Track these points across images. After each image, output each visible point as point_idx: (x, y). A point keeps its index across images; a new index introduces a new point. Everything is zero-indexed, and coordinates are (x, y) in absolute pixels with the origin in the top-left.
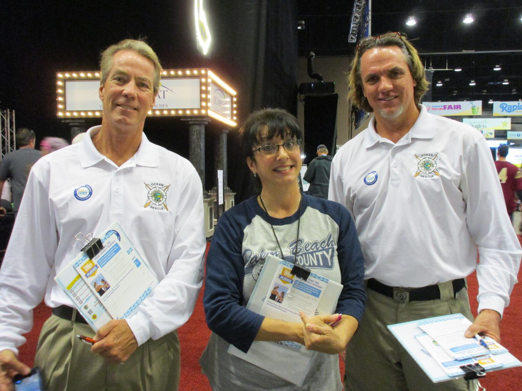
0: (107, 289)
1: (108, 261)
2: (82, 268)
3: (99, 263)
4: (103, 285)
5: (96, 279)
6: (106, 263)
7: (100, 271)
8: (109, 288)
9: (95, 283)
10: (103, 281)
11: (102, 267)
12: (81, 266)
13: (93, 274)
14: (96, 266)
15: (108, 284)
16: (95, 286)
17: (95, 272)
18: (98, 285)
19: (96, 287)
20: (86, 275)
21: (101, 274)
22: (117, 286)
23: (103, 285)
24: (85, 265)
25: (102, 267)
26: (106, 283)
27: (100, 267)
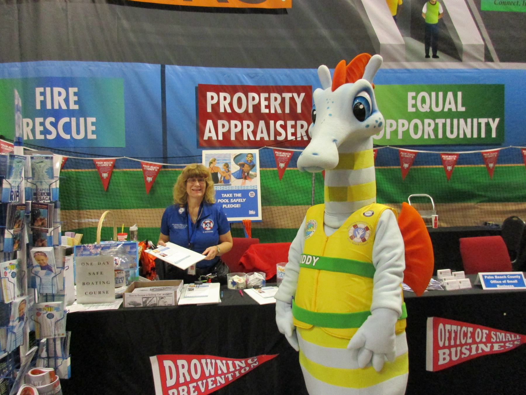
9: (215, 160)
18: (217, 165)
19: (212, 165)
26: (229, 171)
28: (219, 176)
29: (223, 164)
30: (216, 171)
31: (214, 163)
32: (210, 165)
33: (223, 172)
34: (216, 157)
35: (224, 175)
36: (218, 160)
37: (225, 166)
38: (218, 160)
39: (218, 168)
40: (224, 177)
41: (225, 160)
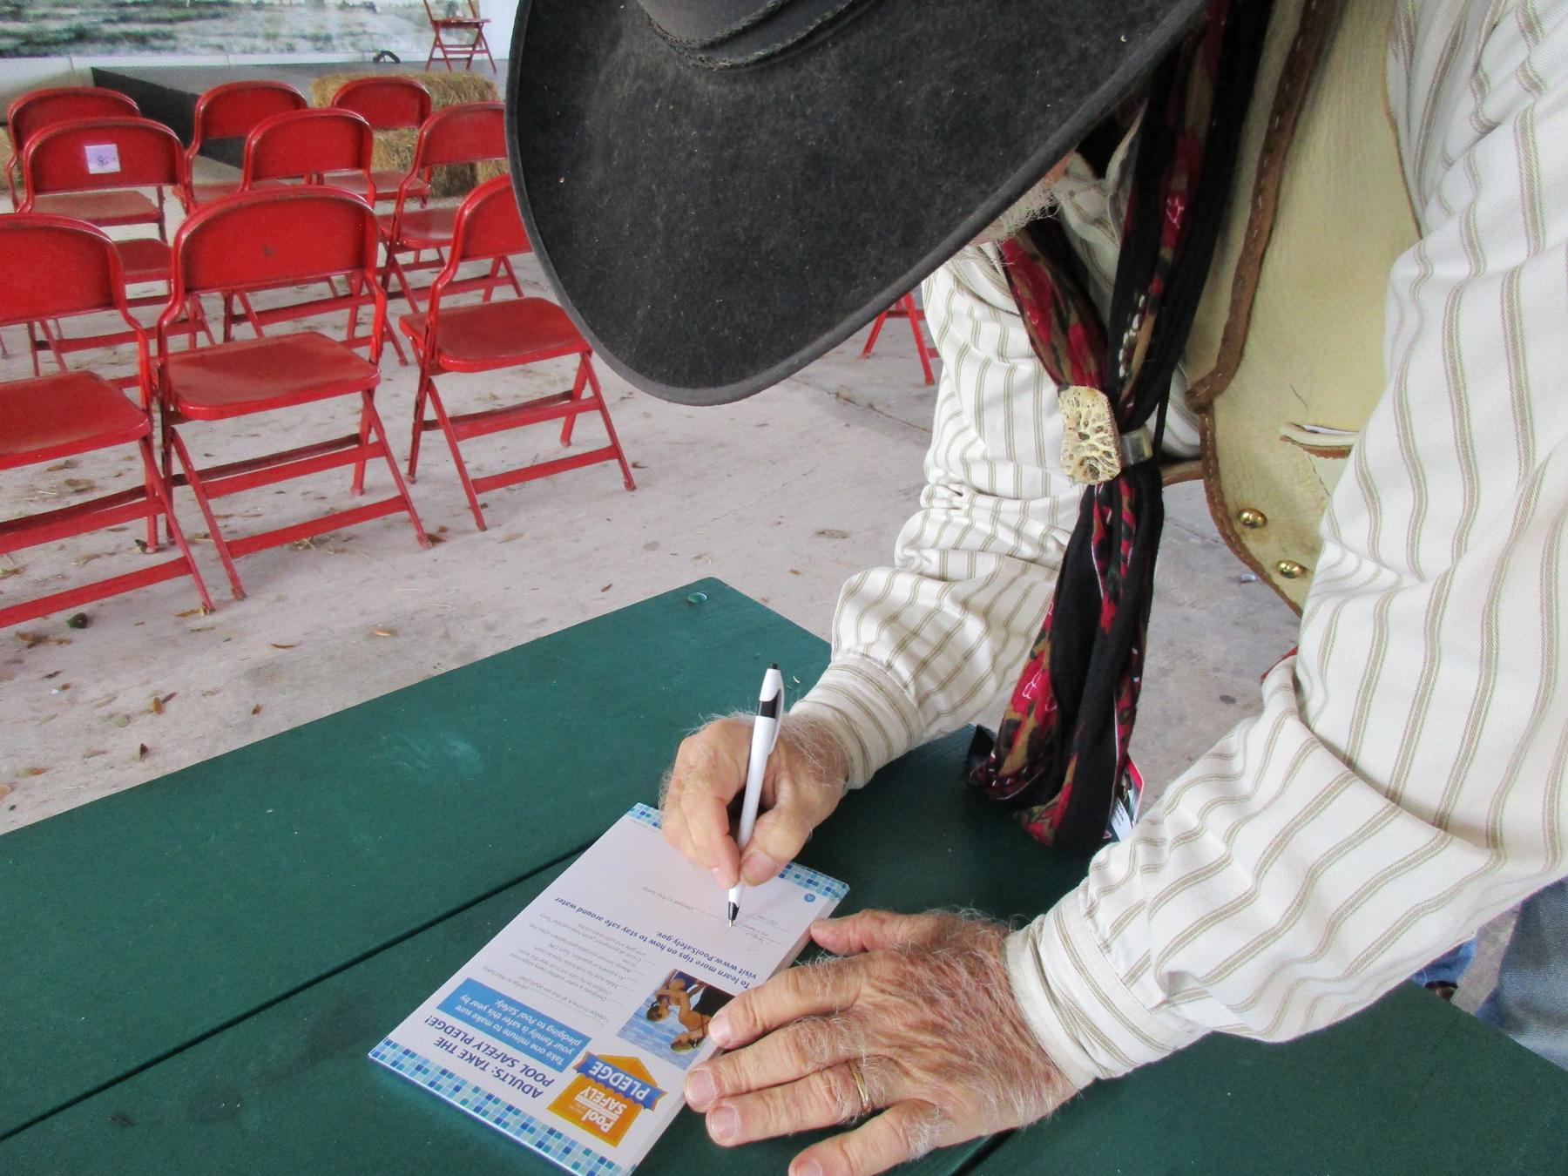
0: (689, 980)
1: (549, 1021)
2: (614, 1136)
3: (566, 1064)
4: (675, 1008)
5: (654, 1049)
6: (560, 1027)
7: (607, 1042)
8: (681, 975)
9: (677, 1045)
10: (654, 1013)
11: (585, 1040)
12: (600, 1147)
13: (633, 1068)
14: (584, 1068)
15: (667, 985)
16: (693, 1043)
17: (616, 1064)
19: (696, 1035)
20: (649, 1103)
21: (623, 1033)
22: (662, 942)
23: (675, 1008)
24: (592, 1127)
25: (585, 1040)
26: (660, 998)
27: (589, 1048)
28: (695, 999)
29: (660, 1022)
30: (697, 1015)
31: (685, 1039)
32: (699, 1041)
33: (678, 1002)
34: (669, 1051)
35: (682, 994)
36: (666, 1039)
37: (660, 1016)
38: (666, 1039)
39: (683, 1021)
40: (685, 989)
41: (645, 1029)
